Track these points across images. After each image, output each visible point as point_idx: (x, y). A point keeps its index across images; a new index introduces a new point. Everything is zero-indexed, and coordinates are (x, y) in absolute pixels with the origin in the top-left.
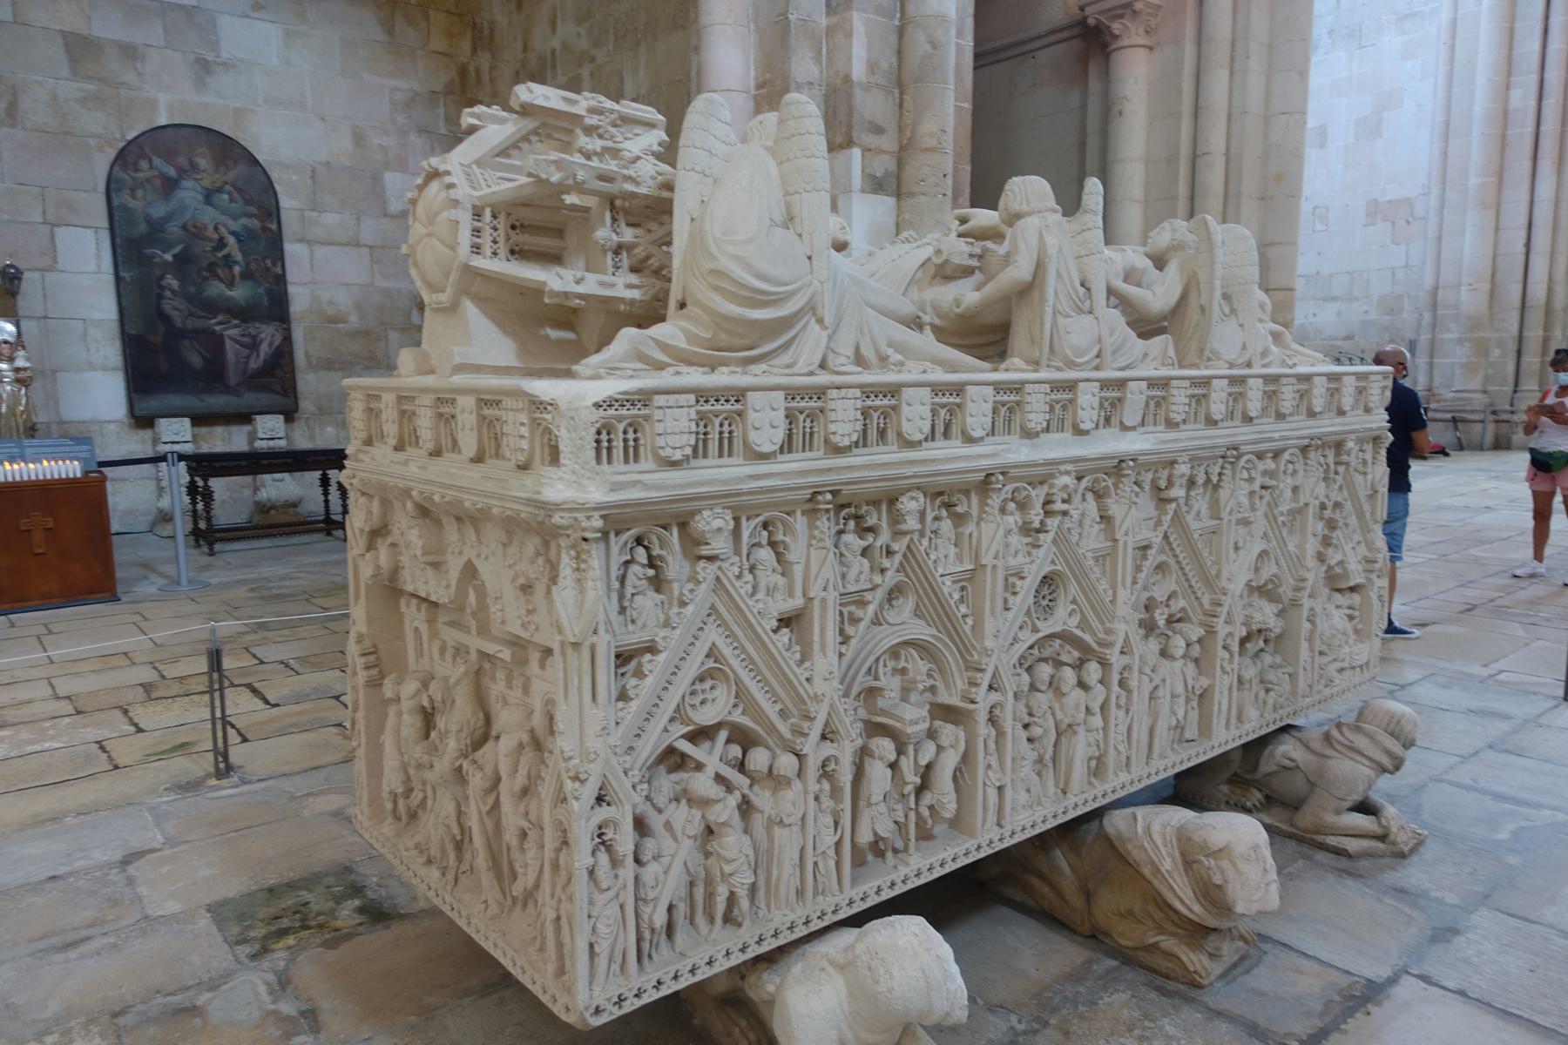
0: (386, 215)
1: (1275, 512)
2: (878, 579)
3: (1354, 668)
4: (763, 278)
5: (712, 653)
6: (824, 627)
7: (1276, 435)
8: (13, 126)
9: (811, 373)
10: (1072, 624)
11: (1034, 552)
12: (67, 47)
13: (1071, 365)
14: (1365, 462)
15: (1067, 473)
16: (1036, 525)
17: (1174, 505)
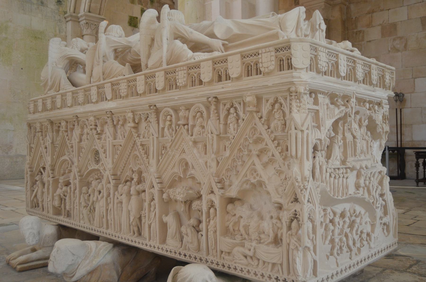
3: (269, 263)
7: (176, 98)
9: (45, 94)
10: (101, 169)
14: (284, 113)
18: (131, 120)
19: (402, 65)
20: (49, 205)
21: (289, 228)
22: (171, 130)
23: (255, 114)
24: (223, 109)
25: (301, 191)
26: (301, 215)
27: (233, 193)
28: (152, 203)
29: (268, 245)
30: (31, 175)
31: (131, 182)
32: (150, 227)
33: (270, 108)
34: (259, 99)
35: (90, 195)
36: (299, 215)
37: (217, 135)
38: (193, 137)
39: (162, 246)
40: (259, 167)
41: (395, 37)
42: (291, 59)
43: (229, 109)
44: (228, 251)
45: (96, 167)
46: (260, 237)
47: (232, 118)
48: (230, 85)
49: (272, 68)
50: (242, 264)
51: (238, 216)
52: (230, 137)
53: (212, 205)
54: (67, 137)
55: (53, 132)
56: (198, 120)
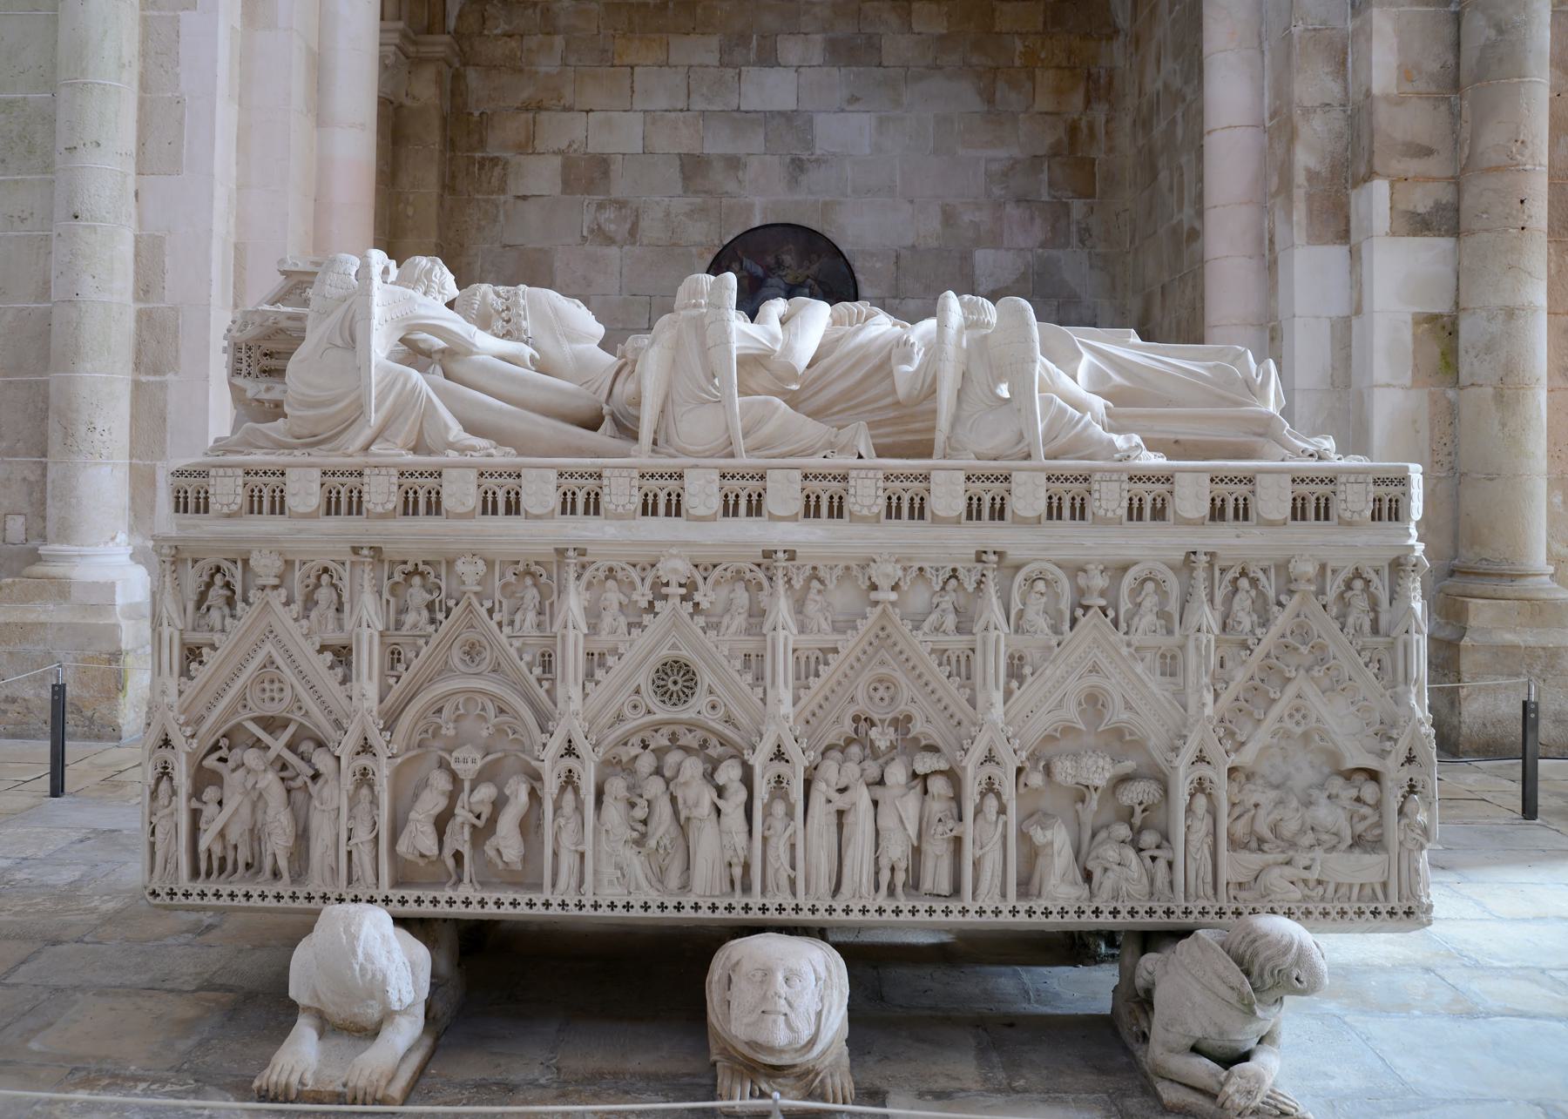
1: (1112, 638)
3: (1351, 886)
6: (368, 658)
9: (350, 456)
16: (644, 604)
17: (880, 608)
20: (364, 858)
27: (1246, 758)
32: (977, 864)
34: (1323, 567)
38: (1135, 639)
40: (1317, 703)
43: (1237, 579)
45: (686, 713)
47: (1243, 602)
48: (1256, 531)
52: (1250, 642)
53: (1200, 787)
54: (497, 617)
56: (1148, 599)
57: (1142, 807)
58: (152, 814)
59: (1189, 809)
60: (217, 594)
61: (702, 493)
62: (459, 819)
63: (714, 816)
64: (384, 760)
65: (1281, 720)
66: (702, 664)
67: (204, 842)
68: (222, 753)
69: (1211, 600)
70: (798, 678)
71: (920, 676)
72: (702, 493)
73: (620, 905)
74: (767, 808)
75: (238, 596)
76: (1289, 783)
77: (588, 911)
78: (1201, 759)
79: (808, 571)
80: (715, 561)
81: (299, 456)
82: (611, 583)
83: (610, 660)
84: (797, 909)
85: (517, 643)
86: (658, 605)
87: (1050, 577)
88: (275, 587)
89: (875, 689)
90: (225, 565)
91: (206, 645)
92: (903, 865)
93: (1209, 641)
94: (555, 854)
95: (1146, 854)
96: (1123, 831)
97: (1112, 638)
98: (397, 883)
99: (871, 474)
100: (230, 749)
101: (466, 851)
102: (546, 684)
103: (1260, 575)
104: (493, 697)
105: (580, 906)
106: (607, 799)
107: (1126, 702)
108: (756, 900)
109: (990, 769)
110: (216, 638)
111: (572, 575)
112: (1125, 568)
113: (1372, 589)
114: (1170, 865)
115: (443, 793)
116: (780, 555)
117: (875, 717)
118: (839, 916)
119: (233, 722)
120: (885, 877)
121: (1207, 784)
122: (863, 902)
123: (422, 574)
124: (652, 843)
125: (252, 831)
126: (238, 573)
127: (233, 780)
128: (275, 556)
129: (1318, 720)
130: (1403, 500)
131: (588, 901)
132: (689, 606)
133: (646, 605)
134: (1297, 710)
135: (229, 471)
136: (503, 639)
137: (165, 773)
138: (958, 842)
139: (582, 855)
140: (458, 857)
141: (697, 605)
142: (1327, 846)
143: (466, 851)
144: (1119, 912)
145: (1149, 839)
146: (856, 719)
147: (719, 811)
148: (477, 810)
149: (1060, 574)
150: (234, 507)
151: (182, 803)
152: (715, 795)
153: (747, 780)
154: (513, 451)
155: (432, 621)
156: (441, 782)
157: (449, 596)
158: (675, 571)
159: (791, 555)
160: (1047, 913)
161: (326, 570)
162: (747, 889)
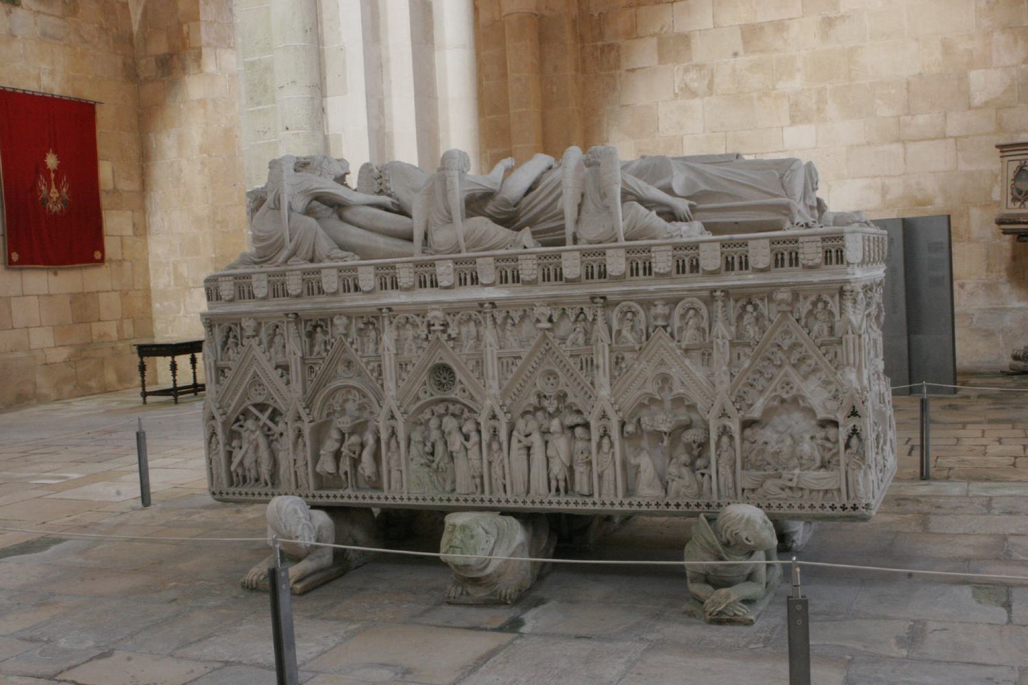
0: (970, 108)
2: (324, 354)
3: (819, 491)
4: (260, 231)
5: (255, 375)
7: (652, 288)
8: (711, 95)
9: (278, 266)
11: (420, 351)
12: (742, 33)
13: (437, 252)
14: (831, 313)
15: (438, 309)
16: (424, 336)
18: (544, 319)
19: (704, 127)
20: (301, 472)
21: (847, 446)
22: (634, 333)
23: (790, 315)
24: (734, 307)
25: (863, 403)
26: (863, 429)
27: (756, 414)
28: (606, 441)
29: (814, 470)
30: (224, 423)
31: (534, 415)
32: (600, 477)
33: (811, 307)
34: (796, 296)
35: (433, 446)
36: (861, 430)
37: (730, 341)
39: (630, 499)
40: (796, 378)
41: (687, 64)
42: (842, 251)
44: (752, 487)
46: (800, 464)
47: (748, 318)
48: (751, 276)
49: (818, 261)
50: (778, 499)
51: (761, 441)
52: (752, 344)
53: (725, 431)
54: (354, 346)
55: (300, 337)
57: (696, 444)
58: (209, 453)
59: (718, 446)
60: (231, 340)
61: (446, 273)
62: (344, 454)
63: (464, 453)
64: (306, 423)
65: (775, 390)
66: (455, 368)
67: (233, 468)
68: (241, 423)
69: (727, 319)
70: (503, 374)
71: (568, 370)
72: (446, 273)
73: (420, 498)
74: (489, 446)
75: (239, 342)
76: (789, 431)
77: (405, 502)
78: (724, 414)
79: (504, 314)
80: (457, 311)
81: (257, 268)
82: (408, 326)
83: (409, 368)
84: (507, 501)
85: (364, 360)
86: (430, 336)
87: (633, 310)
88: (254, 337)
89: (549, 379)
90: (233, 326)
91: (227, 368)
92: (561, 477)
93: (724, 344)
94: (390, 472)
95: (698, 472)
96: (684, 458)
97: (671, 344)
98: (320, 487)
99: (529, 256)
100: (245, 420)
101: (348, 470)
102: (380, 382)
103: (758, 302)
104: (359, 390)
105: (402, 499)
106: (412, 442)
107: (683, 383)
108: (487, 496)
109: (604, 422)
110: (230, 364)
111: (387, 322)
112: (676, 304)
113: (829, 307)
114: (710, 477)
115: (337, 440)
116: (486, 305)
117: (547, 394)
118: (529, 505)
119: (242, 408)
120: (554, 484)
121: (728, 429)
122: (541, 498)
123: (321, 327)
124: (434, 465)
125: (256, 461)
126: (239, 330)
127: (245, 435)
128: (252, 320)
129: (798, 390)
130: (844, 250)
131: (405, 496)
132: (445, 336)
133: (425, 337)
134: (787, 384)
135: (227, 278)
136: (358, 358)
137: (213, 434)
138: (590, 463)
139: (401, 471)
140: (346, 473)
141: (449, 335)
142: (806, 467)
143: (348, 470)
144: (680, 505)
145: (699, 463)
146: (539, 396)
147: (466, 449)
148: (353, 448)
149: (639, 307)
150: (231, 297)
151: (221, 447)
152: (463, 439)
153: (479, 432)
154: (357, 257)
155: (326, 350)
156: (335, 435)
157: (333, 337)
158: (435, 317)
159: (493, 304)
160: (640, 505)
161: (277, 327)
162: (483, 492)
